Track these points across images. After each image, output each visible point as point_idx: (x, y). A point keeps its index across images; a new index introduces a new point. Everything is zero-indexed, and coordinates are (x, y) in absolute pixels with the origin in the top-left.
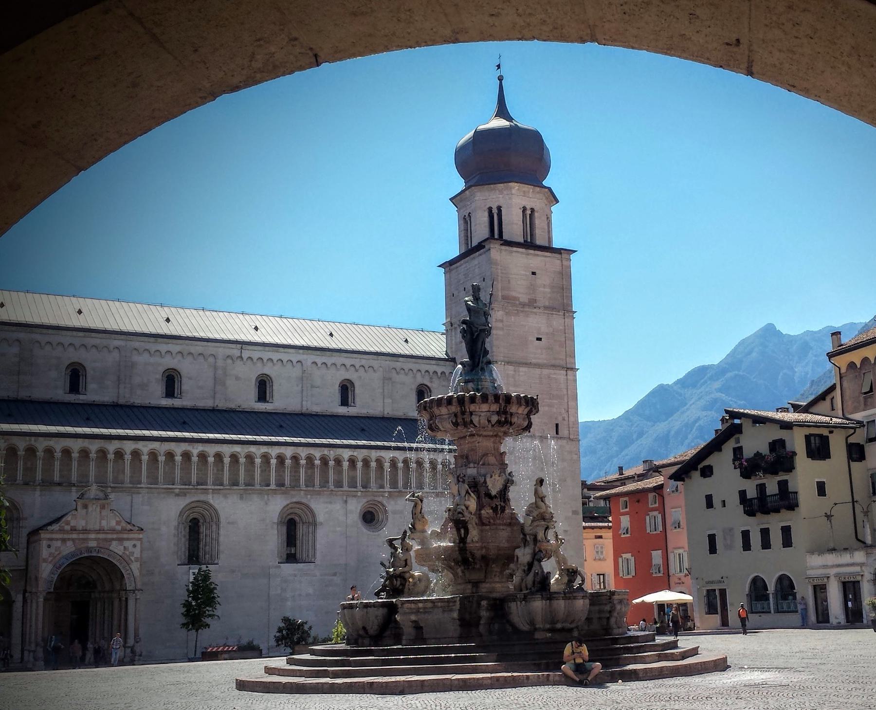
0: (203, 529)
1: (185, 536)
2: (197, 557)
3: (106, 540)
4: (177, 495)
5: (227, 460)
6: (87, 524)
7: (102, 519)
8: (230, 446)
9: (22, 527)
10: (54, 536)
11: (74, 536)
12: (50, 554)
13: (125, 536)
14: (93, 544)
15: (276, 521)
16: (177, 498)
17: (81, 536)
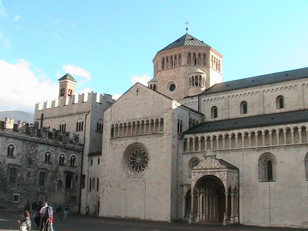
0: (273, 164)
1: (264, 169)
2: (272, 179)
3: (214, 172)
4: (257, 151)
5: (277, 132)
6: (206, 166)
7: (212, 163)
8: (278, 126)
10: (196, 171)
11: (202, 171)
12: (195, 178)
13: (220, 170)
14: (209, 174)
15: (304, 160)
16: (257, 152)
17: (205, 171)
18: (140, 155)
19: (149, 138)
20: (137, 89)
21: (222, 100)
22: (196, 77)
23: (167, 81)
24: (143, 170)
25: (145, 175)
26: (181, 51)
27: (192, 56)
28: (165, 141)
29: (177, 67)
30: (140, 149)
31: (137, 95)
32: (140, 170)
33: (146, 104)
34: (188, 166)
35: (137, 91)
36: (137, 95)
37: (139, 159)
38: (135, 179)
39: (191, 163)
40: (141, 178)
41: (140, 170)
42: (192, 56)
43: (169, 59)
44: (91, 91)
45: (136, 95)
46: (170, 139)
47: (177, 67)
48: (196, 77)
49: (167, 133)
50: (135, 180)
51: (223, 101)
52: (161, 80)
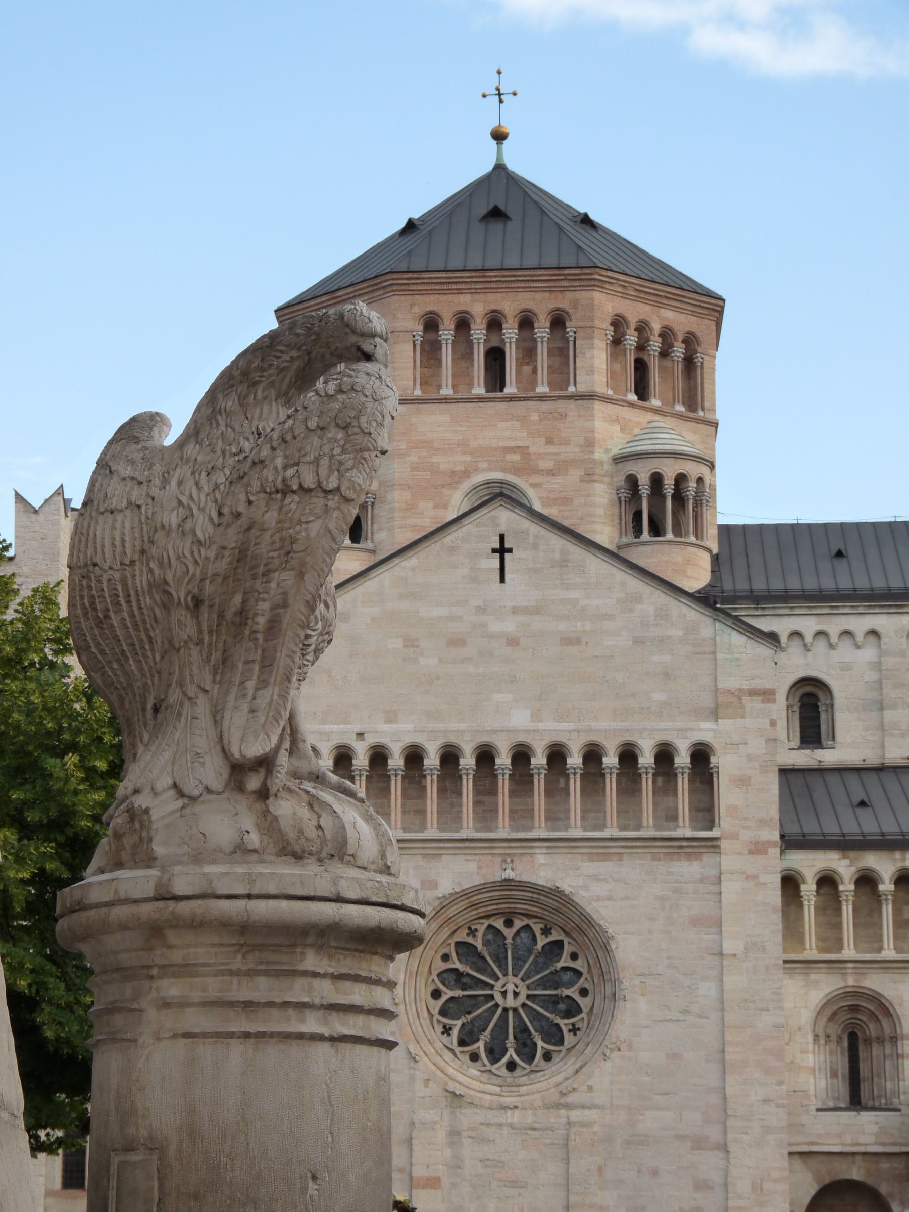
9: (903, 1057)
18: (519, 961)
19: (605, 857)
20: (498, 538)
21: (858, 647)
22: (681, 479)
23: (466, 474)
24: (547, 1056)
25: (590, 1088)
26: (569, 295)
27: (631, 339)
28: (731, 888)
29: (542, 398)
30: (518, 923)
31: (502, 580)
32: (530, 1057)
33: (569, 641)
34: (810, 1038)
35: (502, 551)
36: (502, 580)
37: (510, 987)
38: (515, 1117)
39: (823, 1021)
40: (558, 1106)
41: (530, 1058)
42: (631, 339)
43: (478, 332)
44: (59, 485)
45: (497, 577)
46: (763, 879)
47: (542, 398)
48: (681, 479)
49: (746, 836)
50: (515, 1120)
51: (868, 654)
52: (413, 458)
